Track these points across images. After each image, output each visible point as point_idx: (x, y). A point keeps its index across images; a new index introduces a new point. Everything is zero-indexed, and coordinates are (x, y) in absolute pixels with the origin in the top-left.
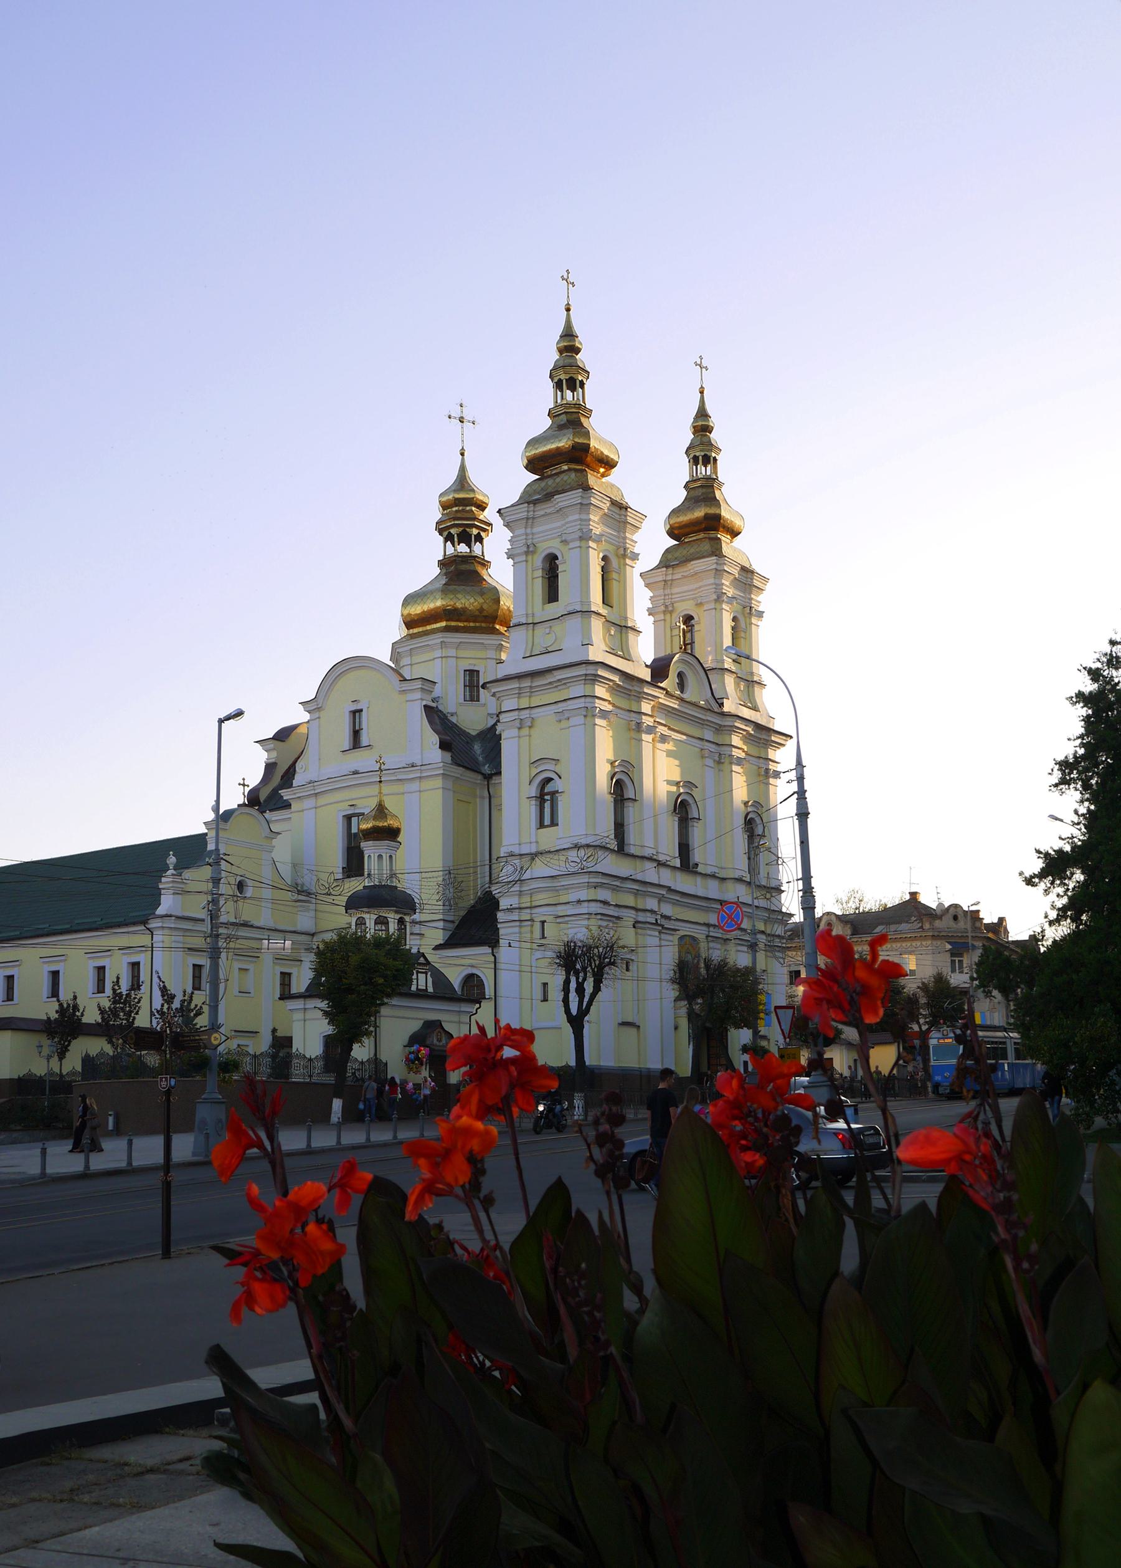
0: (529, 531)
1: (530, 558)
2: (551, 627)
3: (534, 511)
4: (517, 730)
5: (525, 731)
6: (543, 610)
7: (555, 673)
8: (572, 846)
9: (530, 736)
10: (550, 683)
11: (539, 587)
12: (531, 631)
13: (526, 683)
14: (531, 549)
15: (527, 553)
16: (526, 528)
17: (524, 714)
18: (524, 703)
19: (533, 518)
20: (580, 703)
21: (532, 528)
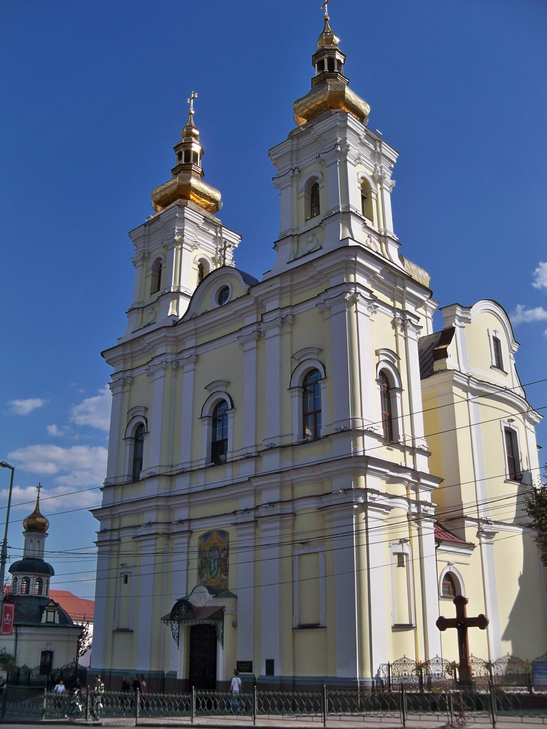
0: (147, 244)
1: (145, 264)
2: (153, 309)
3: (149, 230)
4: (121, 387)
5: (127, 388)
6: (150, 298)
7: (146, 338)
8: (148, 475)
9: (130, 390)
10: (144, 347)
11: (149, 283)
12: (140, 315)
13: (128, 350)
14: (146, 255)
15: (144, 258)
16: (145, 243)
17: (128, 374)
18: (129, 367)
19: (149, 235)
20: (163, 358)
21: (149, 243)
